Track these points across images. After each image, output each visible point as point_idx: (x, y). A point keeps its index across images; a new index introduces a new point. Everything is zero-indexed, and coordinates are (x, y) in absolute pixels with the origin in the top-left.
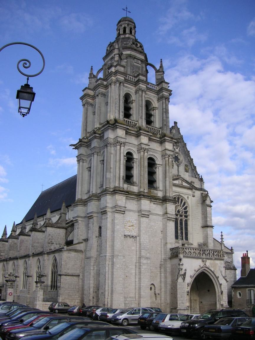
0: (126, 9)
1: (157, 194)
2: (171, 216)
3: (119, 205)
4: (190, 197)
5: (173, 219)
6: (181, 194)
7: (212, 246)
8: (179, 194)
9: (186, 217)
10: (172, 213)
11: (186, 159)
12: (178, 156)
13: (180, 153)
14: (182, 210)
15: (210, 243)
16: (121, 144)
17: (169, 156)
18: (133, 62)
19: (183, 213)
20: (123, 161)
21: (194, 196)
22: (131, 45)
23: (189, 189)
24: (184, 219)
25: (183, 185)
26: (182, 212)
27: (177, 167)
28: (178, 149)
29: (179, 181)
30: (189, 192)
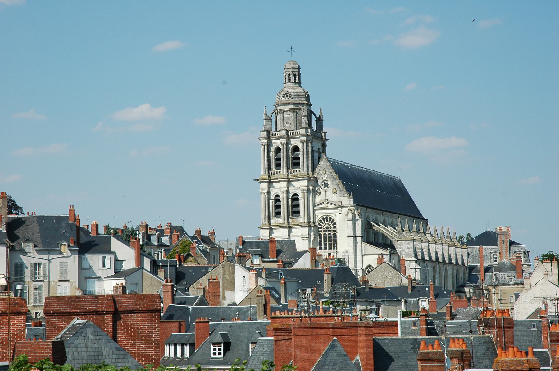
0: (290, 50)
1: (299, 221)
2: (304, 237)
3: (264, 236)
4: (338, 214)
5: (306, 238)
6: (328, 214)
7: (351, 252)
8: (326, 214)
9: (335, 231)
10: (305, 234)
11: (334, 183)
12: (327, 182)
13: (328, 180)
14: (331, 226)
15: (350, 250)
16: (265, 193)
17: (304, 191)
18: (283, 116)
19: (332, 228)
20: (272, 203)
21: (341, 213)
22: (282, 99)
23: (335, 208)
24: (332, 233)
25: (329, 206)
26: (331, 228)
27: (325, 192)
28: (326, 176)
29: (324, 204)
30: (337, 211)
